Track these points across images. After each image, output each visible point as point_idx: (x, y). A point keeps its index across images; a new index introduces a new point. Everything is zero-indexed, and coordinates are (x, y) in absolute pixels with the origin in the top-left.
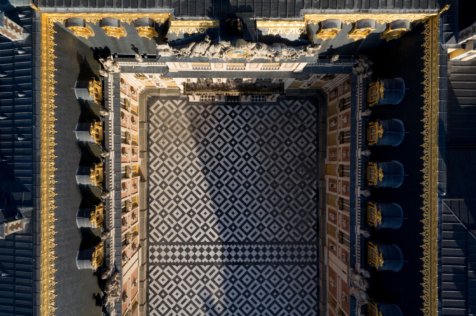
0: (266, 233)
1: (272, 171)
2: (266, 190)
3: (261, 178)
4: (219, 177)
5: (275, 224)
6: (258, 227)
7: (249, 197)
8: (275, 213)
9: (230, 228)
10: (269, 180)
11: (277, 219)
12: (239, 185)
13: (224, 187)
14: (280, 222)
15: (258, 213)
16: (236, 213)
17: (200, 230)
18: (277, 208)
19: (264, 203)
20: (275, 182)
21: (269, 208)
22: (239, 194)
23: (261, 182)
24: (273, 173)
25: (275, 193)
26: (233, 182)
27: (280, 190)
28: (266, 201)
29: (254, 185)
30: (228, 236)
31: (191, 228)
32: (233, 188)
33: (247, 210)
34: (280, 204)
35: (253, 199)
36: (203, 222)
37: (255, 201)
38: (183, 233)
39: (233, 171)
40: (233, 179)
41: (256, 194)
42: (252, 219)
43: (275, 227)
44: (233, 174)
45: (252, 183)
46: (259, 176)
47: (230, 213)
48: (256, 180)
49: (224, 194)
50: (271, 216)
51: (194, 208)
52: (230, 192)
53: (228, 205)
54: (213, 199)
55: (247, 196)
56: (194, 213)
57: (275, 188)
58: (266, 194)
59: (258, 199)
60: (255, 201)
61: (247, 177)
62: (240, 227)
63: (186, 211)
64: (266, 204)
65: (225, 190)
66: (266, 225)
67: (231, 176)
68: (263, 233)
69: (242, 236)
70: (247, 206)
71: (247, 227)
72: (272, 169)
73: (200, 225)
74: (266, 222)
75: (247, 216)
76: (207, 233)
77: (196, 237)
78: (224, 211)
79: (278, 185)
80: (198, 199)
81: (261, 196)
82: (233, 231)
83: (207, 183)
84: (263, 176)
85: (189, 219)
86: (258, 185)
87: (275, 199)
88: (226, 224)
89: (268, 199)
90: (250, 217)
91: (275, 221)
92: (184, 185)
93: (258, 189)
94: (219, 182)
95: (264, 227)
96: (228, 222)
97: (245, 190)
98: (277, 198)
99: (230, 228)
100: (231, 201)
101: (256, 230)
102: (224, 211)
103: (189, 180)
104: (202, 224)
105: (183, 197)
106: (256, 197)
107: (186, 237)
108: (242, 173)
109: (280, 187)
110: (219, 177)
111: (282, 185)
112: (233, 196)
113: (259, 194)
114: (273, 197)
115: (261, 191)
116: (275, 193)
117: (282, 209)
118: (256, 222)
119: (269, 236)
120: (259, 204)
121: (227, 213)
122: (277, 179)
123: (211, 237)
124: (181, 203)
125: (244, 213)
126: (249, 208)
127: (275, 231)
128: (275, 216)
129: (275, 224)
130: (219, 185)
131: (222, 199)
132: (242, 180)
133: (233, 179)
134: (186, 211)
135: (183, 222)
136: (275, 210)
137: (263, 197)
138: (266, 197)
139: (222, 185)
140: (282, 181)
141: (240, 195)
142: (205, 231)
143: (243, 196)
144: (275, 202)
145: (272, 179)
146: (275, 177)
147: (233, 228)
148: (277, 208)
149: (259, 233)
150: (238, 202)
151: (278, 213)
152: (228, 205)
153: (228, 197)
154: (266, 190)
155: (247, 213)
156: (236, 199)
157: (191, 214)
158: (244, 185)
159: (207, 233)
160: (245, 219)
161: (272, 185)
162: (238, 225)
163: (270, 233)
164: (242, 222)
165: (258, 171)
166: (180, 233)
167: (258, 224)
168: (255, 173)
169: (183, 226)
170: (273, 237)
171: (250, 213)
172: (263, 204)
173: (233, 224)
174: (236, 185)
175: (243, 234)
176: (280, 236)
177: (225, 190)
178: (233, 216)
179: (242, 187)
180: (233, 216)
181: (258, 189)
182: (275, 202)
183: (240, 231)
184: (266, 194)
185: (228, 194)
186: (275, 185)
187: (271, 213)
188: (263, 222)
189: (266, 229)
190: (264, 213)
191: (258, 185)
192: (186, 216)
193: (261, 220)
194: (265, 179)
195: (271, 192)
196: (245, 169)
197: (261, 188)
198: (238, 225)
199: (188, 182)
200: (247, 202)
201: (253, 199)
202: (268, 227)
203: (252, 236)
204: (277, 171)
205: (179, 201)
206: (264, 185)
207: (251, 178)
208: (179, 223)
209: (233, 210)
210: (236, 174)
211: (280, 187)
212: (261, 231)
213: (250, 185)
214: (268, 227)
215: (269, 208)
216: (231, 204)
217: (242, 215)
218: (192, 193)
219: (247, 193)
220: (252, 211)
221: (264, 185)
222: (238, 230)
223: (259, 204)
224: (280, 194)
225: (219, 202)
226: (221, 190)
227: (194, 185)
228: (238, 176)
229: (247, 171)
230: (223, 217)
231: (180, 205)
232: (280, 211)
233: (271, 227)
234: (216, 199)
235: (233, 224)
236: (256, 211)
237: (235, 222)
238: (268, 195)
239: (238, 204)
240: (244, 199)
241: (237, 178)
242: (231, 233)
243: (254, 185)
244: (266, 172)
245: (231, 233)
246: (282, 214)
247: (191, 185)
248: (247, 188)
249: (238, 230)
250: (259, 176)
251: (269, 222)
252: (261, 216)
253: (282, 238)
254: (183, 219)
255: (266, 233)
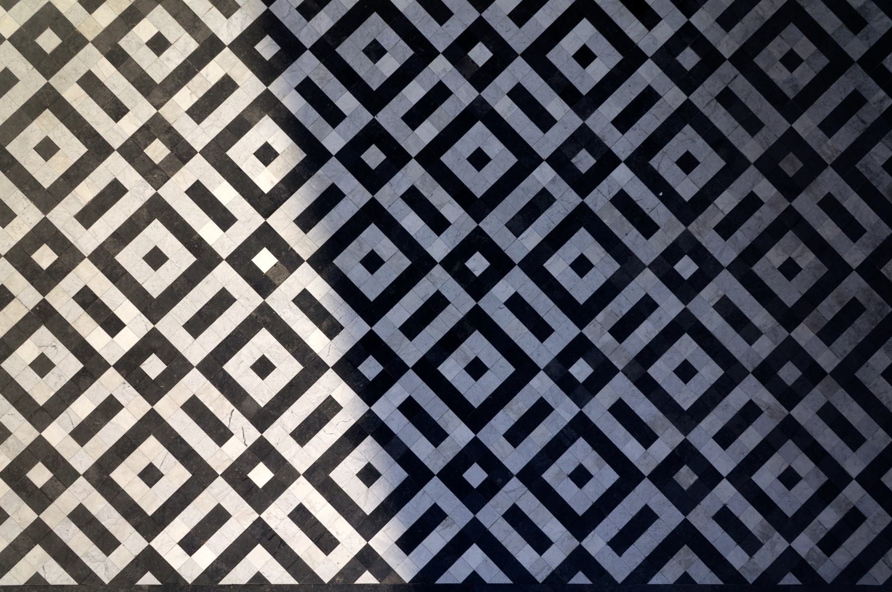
0: (725, 518)
1: (769, 60)
2: (726, 202)
3: (687, 115)
4: (375, 100)
5: (789, 455)
6: (663, 476)
7: (595, 252)
8: (789, 373)
9: (452, 476)
10: (752, 125)
11: (805, 413)
12: (527, 160)
13: (413, 174)
14: (828, 439)
15: (662, 371)
16: (500, 370)
17: (219, 493)
18: (804, 335)
19: (709, 294)
20: (791, 142)
21: (751, 334)
22: (520, 223)
23: (687, 140)
24: (778, 75)
25: (790, 222)
26: (479, 135)
27: (830, 205)
28: (725, 285)
29: (640, 162)
30: (435, 542)
31: (151, 475)
32: (479, 183)
33: (580, 348)
34: (828, 308)
35: (629, 265)
36: (244, 434)
37: (646, 283)
38: (82, 517)
39: (480, 54)
40: (479, 112)
41: (647, 227)
42: (620, 411)
43: (789, 478)
44: (481, 78)
45: (624, 145)
46: (672, 98)
47: (452, 369)
48: (649, 123)
49: (412, 223)
50: (764, 397)
51: (172, 326)
52: (451, 210)
53: (436, 304)
54: (323, 261)
55: (582, 242)
56: (177, 366)
57: (790, 188)
58: (726, 229)
59: (664, 267)
60: (646, 283)
61: (583, 103)
62: (532, 476)
63: (111, 347)
64: (726, 308)
65: (413, 198)
66: (724, 461)
67: (464, 94)
68: (702, 519)
69: (540, 543)
70: (582, 314)
71: (581, 476)
72: (776, 48)
73: (220, 457)
74: (725, 438)
75: (581, 393)
76: (277, 517)
77: (190, 544)
78: (411, 352)
79: (814, 165)
80: (206, 259)
81: (687, 245)
82: (475, 499)
83: (281, 141)
84: (703, 99)
85: (134, 408)
86: (664, 164)
87: (790, 269)
88: (421, 447)
89: (743, 268)
90: (606, 397)
91: (789, 430)
92: (98, 149)
93: (668, 196)
94: (373, 134)
95: (709, 477)
96: (436, 435)
97: (566, 200)
98: (807, 259)
99: (452, 476)
100: (463, 276)
101: (645, 494)
102: (411, 352)
103: (140, 111)
104: (234, 449)
105: (88, 240)
106: (647, 250)
107: (107, 542)
108: (549, 73)
109: (830, 182)
110: (375, 100)
111: (847, 165)
112: (478, 241)
113: (670, 228)
114: (775, 256)
115: (687, 211)
116: (790, 222)
117: (847, 342)
118: (646, 437)
119: (749, 543)
120: (670, 307)
121: (428, 369)
122: (806, 125)
123: (301, 544)
124: (71, 284)
125: (559, 370)
126: (598, 332)
127: (790, 502)
128: (789, 397)
129: (789, 455)
130: (373, 156)
131: (396, 263)
132: (544, 121)
133: (479, 112)
134: (111, 347)
135: (83, 433)
136: (789, 351)
137: (699, 253)
138: (724, 252)
139: (397, 157)
140: (845, 138)
141: (532, 238)
142: (259, 498)
143: (555, 241)
144: (790, 293)
145: (775, 125)
146: (790, 108)
147: (474, 476)
148: (804, 335)
149: (669, 518)
150: (515, 282)
151: (813, 374)
152: (436, 304)
153: (438, 247)
154: (726, 202)
155: (581, 370)
156: (500, 264)
157: (151, 367)
158: (560, 161)
159: (277, 517)
160: (565, 409)
161: (768, 165)
162: (515, 459)
163: (752, 519)
164: (542, 436)
165: (666, 58)
166: (56, 517)
167: (661, 450)
168: (649, 74)
169: (82, 458)
170: (774, 547)
171: (604, 372)
172: (704, 307)
173: (476, 452)
174: (502, 159)
175: (552, 527)
176: (830, 543)
177: (413, 198)
178: (476, 393)
179: (544, 176)
180: (476, 393)
181: (668, 196)
182: (790, 293)
183: (532, 507)
184: (726, 229)
185: (438, 223)
186: (790, 165)
187: (766, 373)
188: (703, 437)
189: (725, 493)
190: (709, 372)
191: (664, 164)
192: (111, 383)
193: (686, 419)
194: (722, 120)
195: (764, 217)
196: (570, 44)
197: (687, 187)
198: (515, 459)
199: (129, 126)
200: (582, 290)
201: (629, 265)
202: (742, 476)
203: (620, 543)
204: (814, 60)
205: (57, 273)
206: (711, 163)
207: (612, 107)
208: (57, 434)
209: (477, 345)
210: (505, 81)
211: (830, 182)
212: (685, 501)
213: (607, 162)
214: (742, 476)
215: (751, 334)
216: (461, 303)
217: (541, 386)
218: (155, 209)
219: (581, 218)
220: (620, 354)
221: (711, 163)
222: (515, 493)
223: (670, 307)
224: (829, 230)
225: (372, 286)
226: (390, 196)
227: (182, 152)
228: (519, 95)
229: (584, 56)
230: (397, 394)
231: (62, 298)
232: (828, 359)
233: (765, 478)
234: (349, 262)
235: (476, 452)
236: (650, 354)
237: (494, 435)
238: (744, 236)
239: (516, 304)
240: (558, 266)
241: (507, 109)
242: (458, 515)
243: (640, 162)
244: (727, 70)
245: (458, 515)
246: (847, 375)
247: (158, 150)
248: (584, 184)
249: (515, 493)
250: (672, 98)
251: (751, 438)
252: (686, 396)
253: (842, 557)
254: (83, 407)
255: (725, 518)
